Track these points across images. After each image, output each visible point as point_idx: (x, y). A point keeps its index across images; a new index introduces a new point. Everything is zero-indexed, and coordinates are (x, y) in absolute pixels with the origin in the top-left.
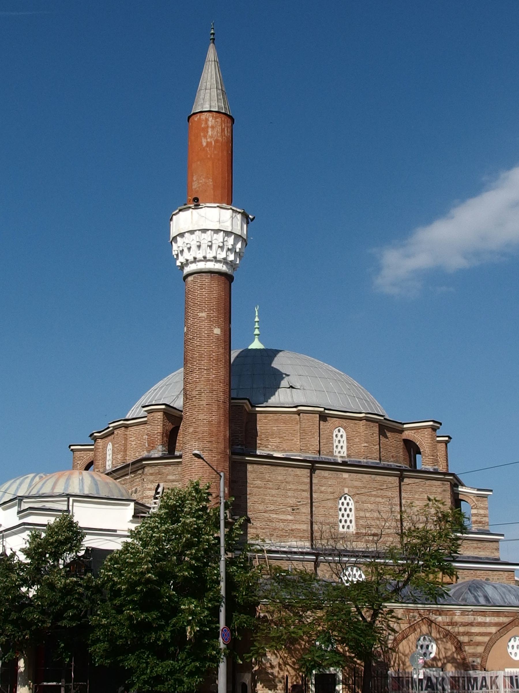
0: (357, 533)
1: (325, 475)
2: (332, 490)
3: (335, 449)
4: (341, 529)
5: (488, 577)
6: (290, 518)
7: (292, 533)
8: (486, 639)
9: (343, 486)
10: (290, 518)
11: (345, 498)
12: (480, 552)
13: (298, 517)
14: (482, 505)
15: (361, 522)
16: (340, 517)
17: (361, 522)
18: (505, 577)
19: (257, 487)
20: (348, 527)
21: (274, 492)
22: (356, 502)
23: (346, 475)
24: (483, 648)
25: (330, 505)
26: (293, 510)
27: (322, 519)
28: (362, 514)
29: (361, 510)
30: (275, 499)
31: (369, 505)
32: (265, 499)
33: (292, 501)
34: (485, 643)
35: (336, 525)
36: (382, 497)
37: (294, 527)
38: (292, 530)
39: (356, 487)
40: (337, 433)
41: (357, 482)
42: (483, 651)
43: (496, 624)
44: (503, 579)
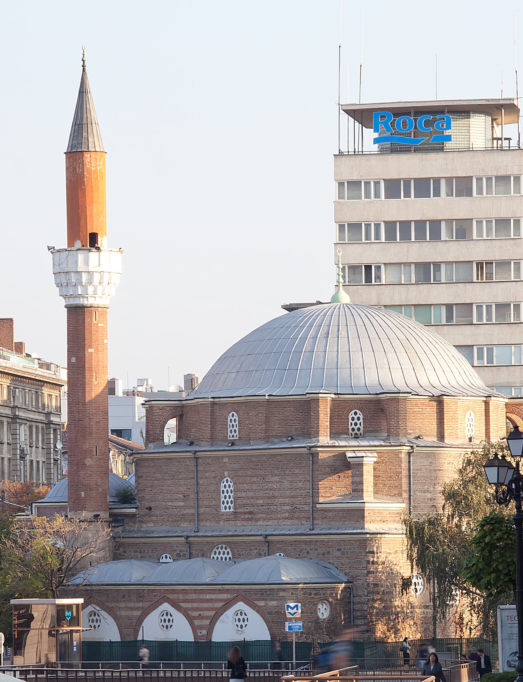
0: (235, 513)
1: (209, 462)
2: (214, 475)
3: (229, 433)
4: (223, 510)
5: (340, 547)
6: (182, 504)
7: (183, 518)
8: (212, 613)
9: (224, 471)
10: (182, 504)
11: (227, 481)
12: (345, 521)
13: (188, 502)
14: (358, 472)
15: (239, 502)
16: (223, 499)
17: (239, 502)
18: (356, 546)
19: (157, 480)
20: (230, 509)
21: (169, 482)
22: (234, 484)
23: (226, 460)
24: (209, 621)
25: (213, 489)
26: (185, 497)
27: (206, 503)
28: (239, 494)
29: (239, 490)
30: (170, 488)
31: (245, 485)
32: (162, 489)
33: (182, 489)
34: (211, 616)
35: (219, 506)
36: (256, 476)
37: (185, 512)
38: (183, 515)
39: (234, 470)
40: (231, 418)
41: (235, 465)
42: (208, 624)
43: (221, 600)
44: (354, 548)
